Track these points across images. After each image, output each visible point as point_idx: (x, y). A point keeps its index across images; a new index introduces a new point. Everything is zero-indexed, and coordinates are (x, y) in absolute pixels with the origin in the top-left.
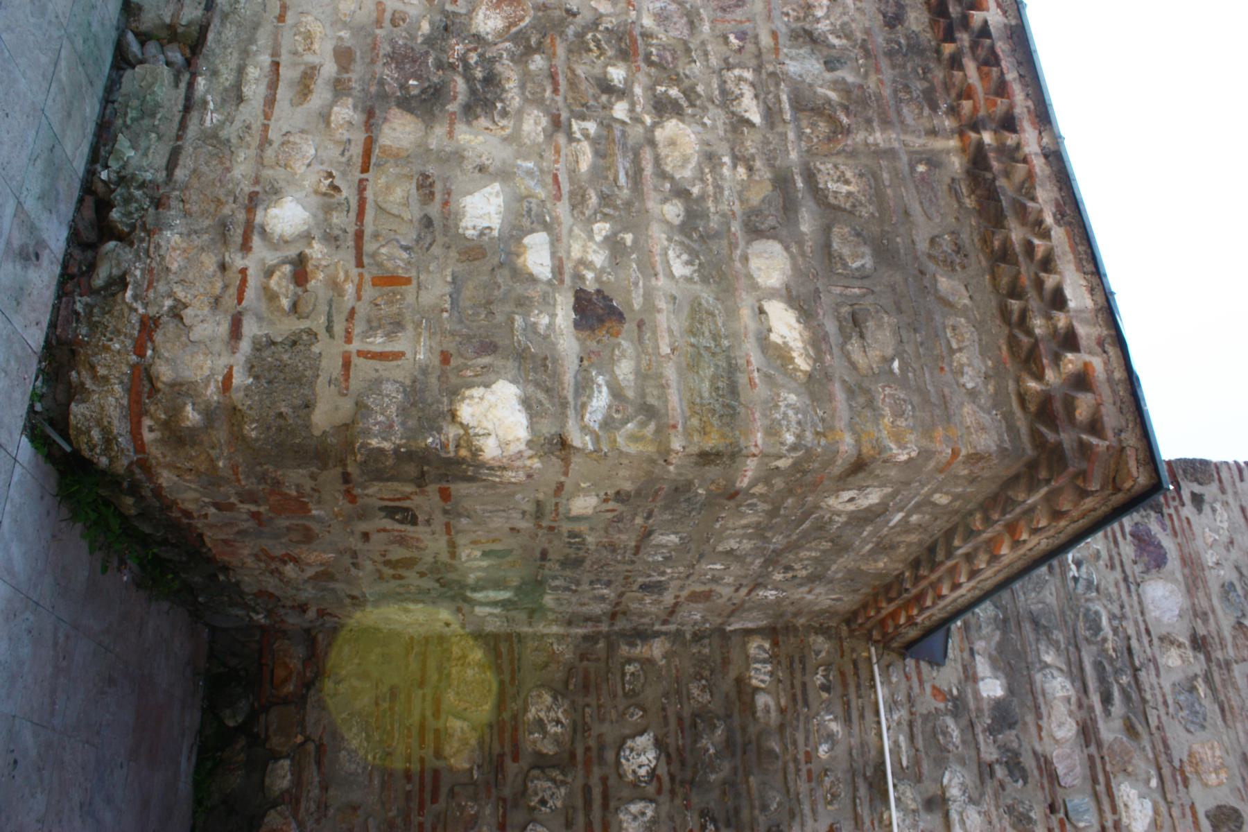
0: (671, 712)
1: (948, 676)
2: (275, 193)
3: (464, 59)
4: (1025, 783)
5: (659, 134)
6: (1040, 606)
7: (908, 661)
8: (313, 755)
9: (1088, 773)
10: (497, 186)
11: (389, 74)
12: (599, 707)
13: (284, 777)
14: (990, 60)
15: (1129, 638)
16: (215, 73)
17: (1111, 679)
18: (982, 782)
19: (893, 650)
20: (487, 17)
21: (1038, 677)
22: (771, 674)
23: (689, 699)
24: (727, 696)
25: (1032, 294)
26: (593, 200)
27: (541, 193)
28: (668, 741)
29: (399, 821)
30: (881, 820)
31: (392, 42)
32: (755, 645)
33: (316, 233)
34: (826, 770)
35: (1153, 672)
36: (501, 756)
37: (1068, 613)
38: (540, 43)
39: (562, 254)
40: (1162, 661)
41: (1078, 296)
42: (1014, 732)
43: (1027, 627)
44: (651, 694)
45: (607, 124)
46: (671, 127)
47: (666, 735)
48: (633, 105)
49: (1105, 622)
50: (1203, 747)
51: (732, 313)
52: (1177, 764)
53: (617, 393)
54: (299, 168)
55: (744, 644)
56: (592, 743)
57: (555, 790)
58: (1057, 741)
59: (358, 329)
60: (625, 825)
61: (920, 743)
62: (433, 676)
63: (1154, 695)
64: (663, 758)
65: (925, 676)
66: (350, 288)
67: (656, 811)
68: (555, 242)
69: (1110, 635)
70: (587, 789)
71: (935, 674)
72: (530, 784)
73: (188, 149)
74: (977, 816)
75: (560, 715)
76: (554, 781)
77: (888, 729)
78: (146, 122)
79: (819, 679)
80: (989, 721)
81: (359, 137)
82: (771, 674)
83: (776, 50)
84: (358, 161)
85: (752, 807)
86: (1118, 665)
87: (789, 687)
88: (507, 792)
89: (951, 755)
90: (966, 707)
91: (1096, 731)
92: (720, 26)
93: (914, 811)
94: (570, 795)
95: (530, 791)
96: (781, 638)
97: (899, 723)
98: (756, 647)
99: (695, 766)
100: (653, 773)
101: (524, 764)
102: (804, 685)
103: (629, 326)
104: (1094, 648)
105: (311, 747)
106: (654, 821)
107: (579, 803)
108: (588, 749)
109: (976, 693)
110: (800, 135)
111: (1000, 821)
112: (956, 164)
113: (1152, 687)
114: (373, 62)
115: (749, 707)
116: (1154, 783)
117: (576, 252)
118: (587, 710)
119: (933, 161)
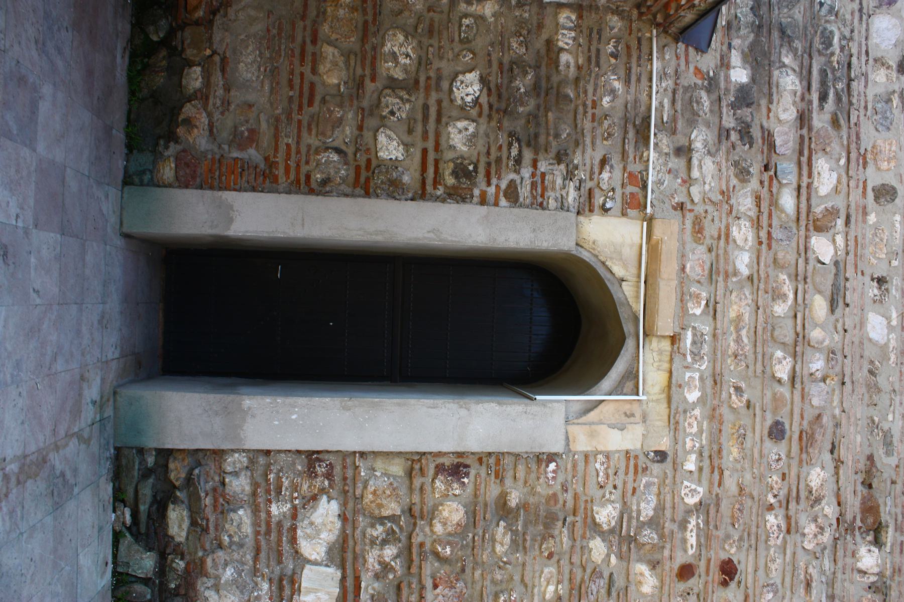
0: (494, 57)
1: (708, 61)
4: (751, 147)
6: (789, 20)
7: (680, 44)
8: (218, 64)
9: (797, 147)
12: (440, 48)
13: (196, 79)
15: (851, 56)
17: (830, 84)
18: (720, 142)
19: (670, 35)
21: (776, 73)
22: (574, 39)
23: (509, 50)
24: (538, 52)
28: (490, 78)
29: (283, 117)
30: (641, 157)
32: (565, 15)
34: (607, 115)
35: (863, 83)
36: (363, 77)
37: (810, 29)
42: (750, 110)
43: (776, 34)
44: (480, 43)
47: (489, 74)
50: (884, 143)
52: (862, 151)
55: (556, 15)
56: (432, 74)
57: (401, 105)
58: (780, 121)
60: (452, 136)
61: (679, 106)
62: (312, 12)
63: (859, 100)
64: (485, 91)
65: (690, 59)
67: (476, 128)
69: (838, 51)
70: (426, 107)
71: (698, 58)
72: (383, 99)
74: (711, 164)
75: (409, 50)
76: (401, 99)
77: (657, 92)
79: (610, 48)
80: (733, 99)
82: (574, 39)
85: (548, 134)
86: (838, 74)
87: (586, 51)
88: (365, 103)
89: (700, 118)
90: (717, 86)
91: (810, 119)
93: (666, 154)
94: (413, 109)
95: (383, 105)
96: (585, 13)
97: (665, 90)
98: (566, 17)
99: (509, 99)
100: (476, 101)
101: (379, 84)
102: (598, 51)
104: (823, 59)
105: (217, 59)
106: (474, 135)
107: (419, 117)
108: (428, 78)
109: (727, 77)
111: (727, 170)
113: (859, 95)
115: (555, 63)
116: (843, 161)
118: (430, 49)
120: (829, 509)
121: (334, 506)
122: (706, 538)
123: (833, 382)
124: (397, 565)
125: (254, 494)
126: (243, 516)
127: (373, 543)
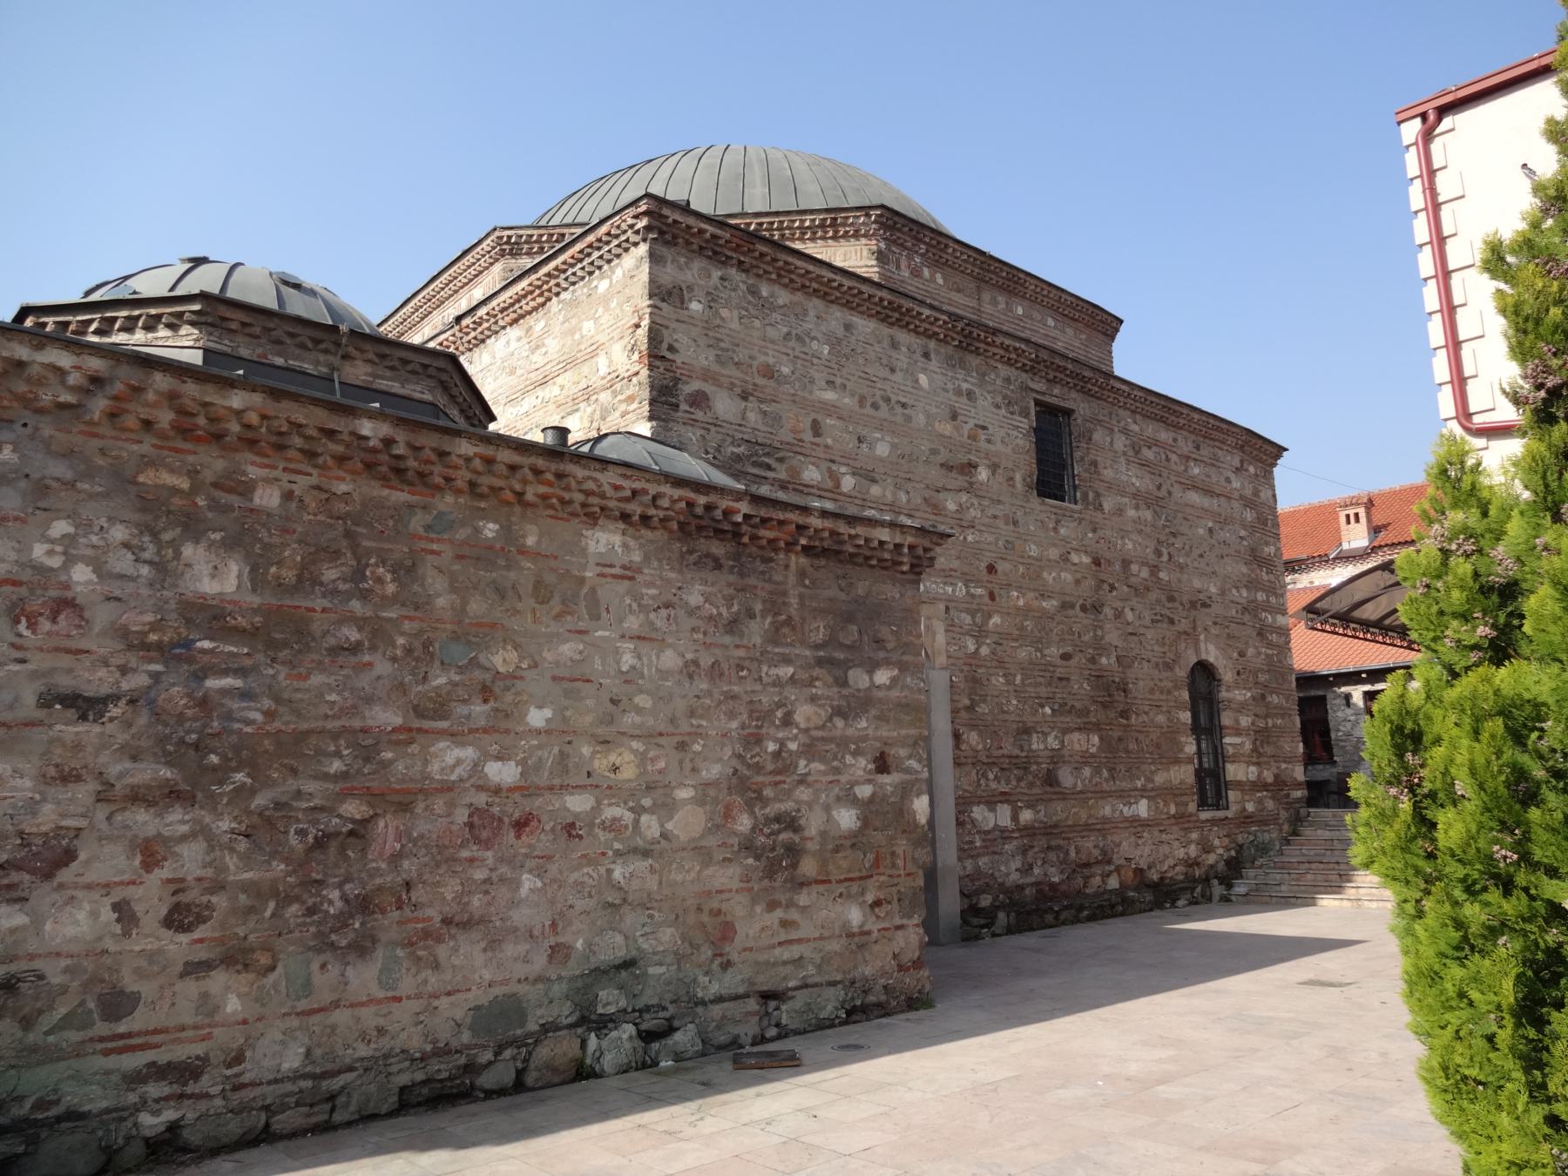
2: (846, 924)
3: (768, 836)
5: (803, 726)
10: (834, 813)
11: (780, 878)
14: (764, 521)
16: (785, 978)
20: (742, 824)
25: (875, 553)
26: (835, 763)
27: (837, 790)
31: (761, 879)
33: (861, 900)
38: (754, 792)
39: (862, 780)
40: (752, 425)
41: (884, 534)
45: (799, 754)
46: (798, 718)
48: (788, 739)
49: (735, 450)
51: (880, 701)
53: (910, 757)
54: (833, 915)
59: (894, 872)
66: (882, 878)
68: (857, 783)
69: (742, 449)
73: (827, 978)
78: (813, 1007)
81: (814, 887)
83: (747, 647)
84: (827, 885)
92: (733, 680)
103: (886, 749)
110: (791, 645)
112: (803, 560)
114: (774, 888)
117: (861, 773)
119: (802, 574)
120: (964, 497)
121: (975, 809)
122: (979, 583)
123: (909, 486)
124: (996, 770)
125: (972, 857)
126: (983, 862)
127: (987, 785)
